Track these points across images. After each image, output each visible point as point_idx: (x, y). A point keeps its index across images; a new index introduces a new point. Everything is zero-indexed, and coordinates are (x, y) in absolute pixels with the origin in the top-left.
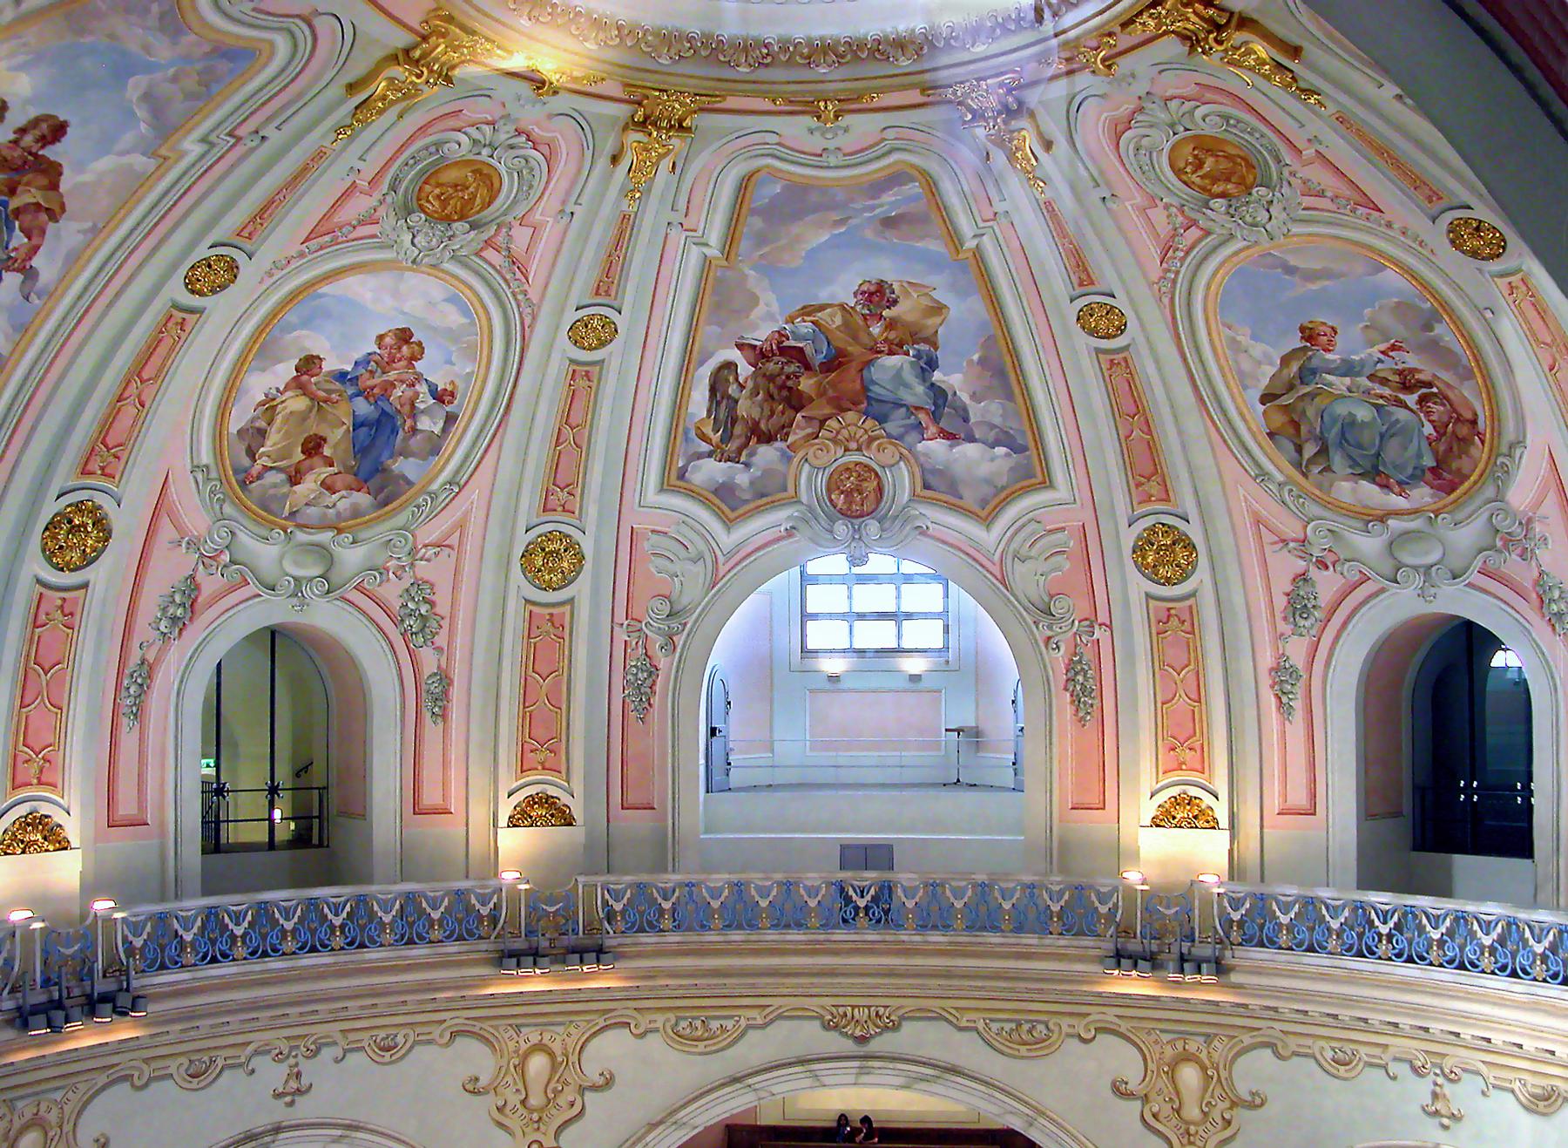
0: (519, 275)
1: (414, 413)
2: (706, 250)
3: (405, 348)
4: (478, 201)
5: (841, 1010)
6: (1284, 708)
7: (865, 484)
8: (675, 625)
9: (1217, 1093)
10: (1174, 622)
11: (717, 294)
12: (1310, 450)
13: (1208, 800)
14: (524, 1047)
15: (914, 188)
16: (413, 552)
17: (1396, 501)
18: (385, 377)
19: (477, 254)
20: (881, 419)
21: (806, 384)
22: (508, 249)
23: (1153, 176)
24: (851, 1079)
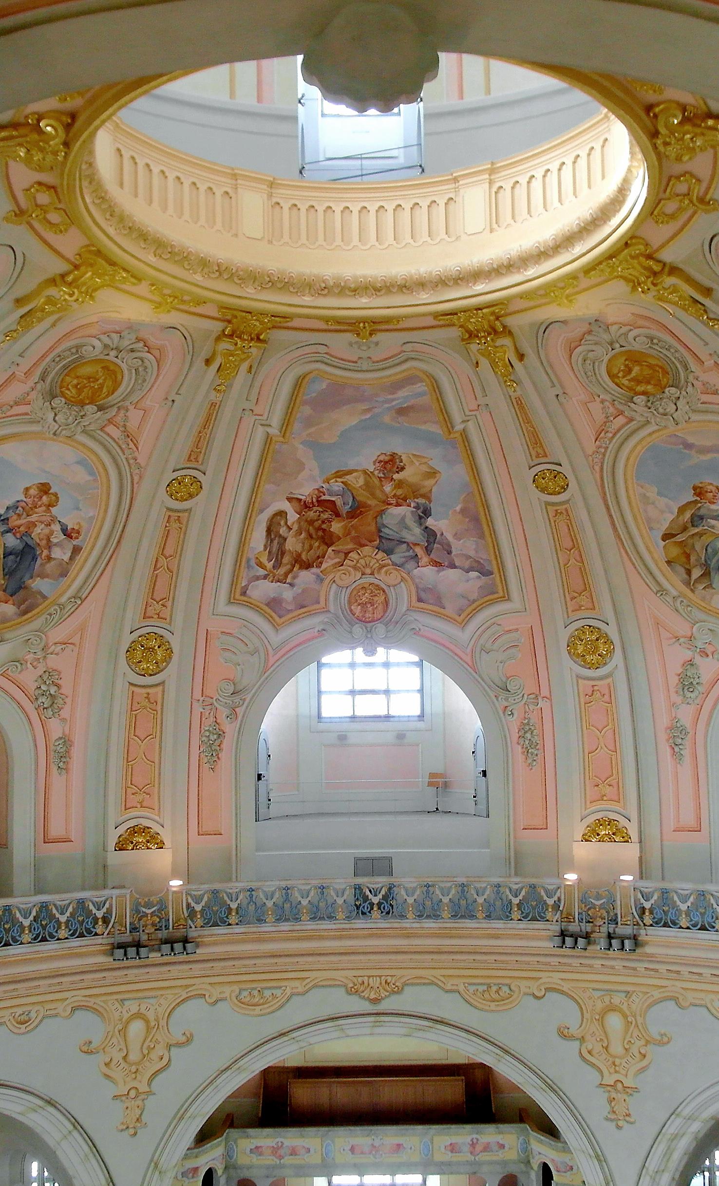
0: (132, 445)
1: (49, 546)
2: (269, 430)
3: (45, 498)
4: (105, 390)
5: (360, 979)
6: (677, 756)
7: (376, 599)
8: (237, 699)
9: (635, 1035)
10: (597, 695)
11: (271, 461)
12: (696, 573)
13: (623, 822)
14: (126, 1016)
18: (29, 519)
19: (101, 430)
20: (389, 552)
21: (336, 527)
22: (125, 426)
23: (594, 379)
24: (368, 1031)
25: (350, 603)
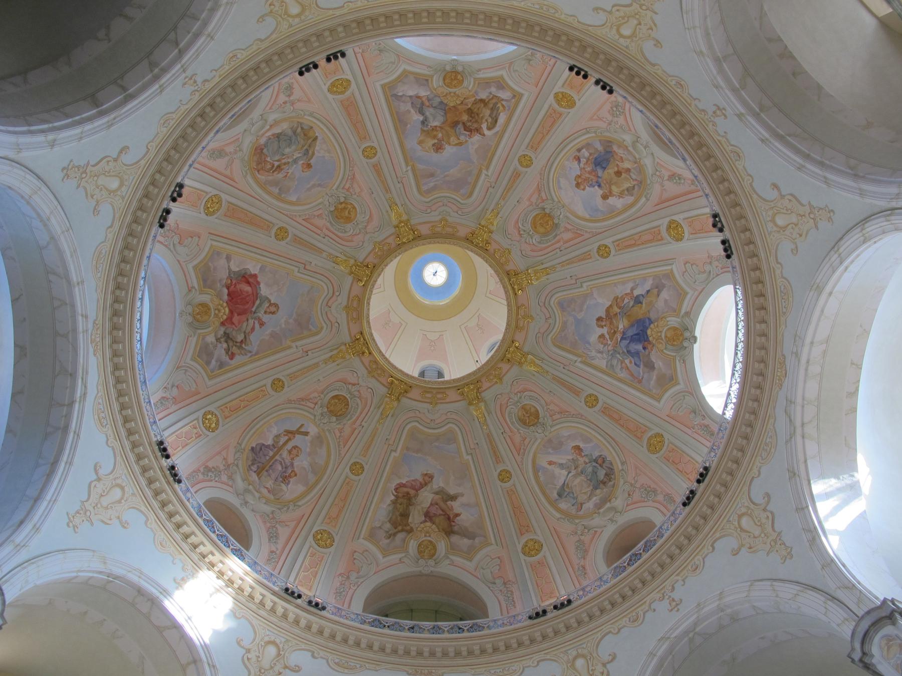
1: (588, 160)
14: (629, 40)
15: (425, 188)
16: (610, 124)
17: (269, 134)
20: (441, 103)
21: (465, 117)
25: (463, 80)
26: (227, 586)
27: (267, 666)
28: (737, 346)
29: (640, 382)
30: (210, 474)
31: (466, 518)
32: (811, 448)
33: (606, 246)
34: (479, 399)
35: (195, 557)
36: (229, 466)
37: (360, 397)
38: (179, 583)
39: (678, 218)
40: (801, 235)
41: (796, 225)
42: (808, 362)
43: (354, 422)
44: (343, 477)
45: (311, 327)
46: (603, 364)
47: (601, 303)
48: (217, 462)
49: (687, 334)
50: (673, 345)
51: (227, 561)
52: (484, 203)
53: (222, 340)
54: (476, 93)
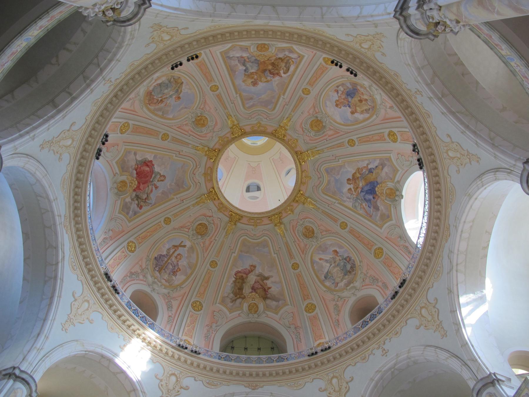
1: (343, 92)
14: (366, 50)
15: (247, 106)
17: (155, 84)
20: (256, 60)
21: (270, 67)
26: (148, 346)
27: (172, 388)
28: (425, 202)
29: (371, 216)
30: (133, 276)
31: (274, 290)
32: (461, 277)
33: (353, 140)
34: (281, 223)
35: (130, 332)
36: (143, 270)
37: (214, 224)
38: (122, 348)
39: (395, 130)
40: (462, 165)
41: (459, 159)
42: (462, 231)
43: (211, 238)
44: (206, 269)
45: (184, 186)
46: (350, 205)
47: (350, 171)
48: (137, 269)
49: (398, 193)
50: (390, 198)
51: (146, 332)
52: (282, 114)
53: (135, 199)
54: (277, 54)
